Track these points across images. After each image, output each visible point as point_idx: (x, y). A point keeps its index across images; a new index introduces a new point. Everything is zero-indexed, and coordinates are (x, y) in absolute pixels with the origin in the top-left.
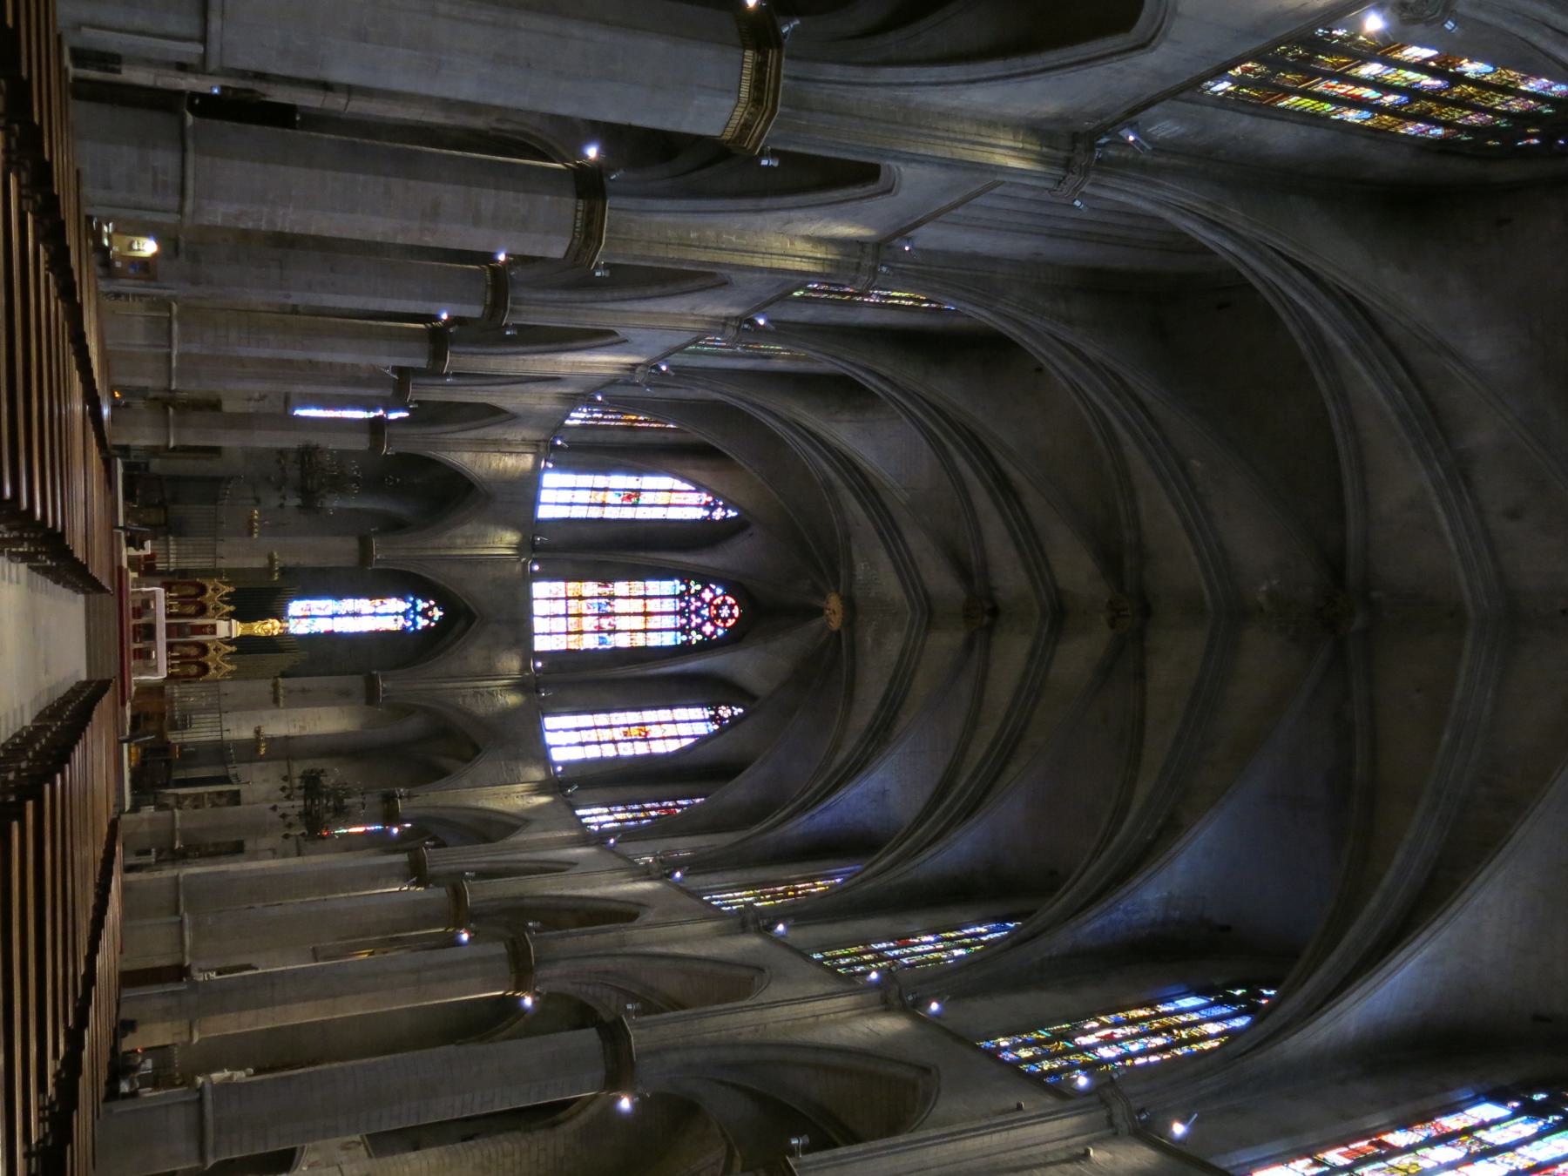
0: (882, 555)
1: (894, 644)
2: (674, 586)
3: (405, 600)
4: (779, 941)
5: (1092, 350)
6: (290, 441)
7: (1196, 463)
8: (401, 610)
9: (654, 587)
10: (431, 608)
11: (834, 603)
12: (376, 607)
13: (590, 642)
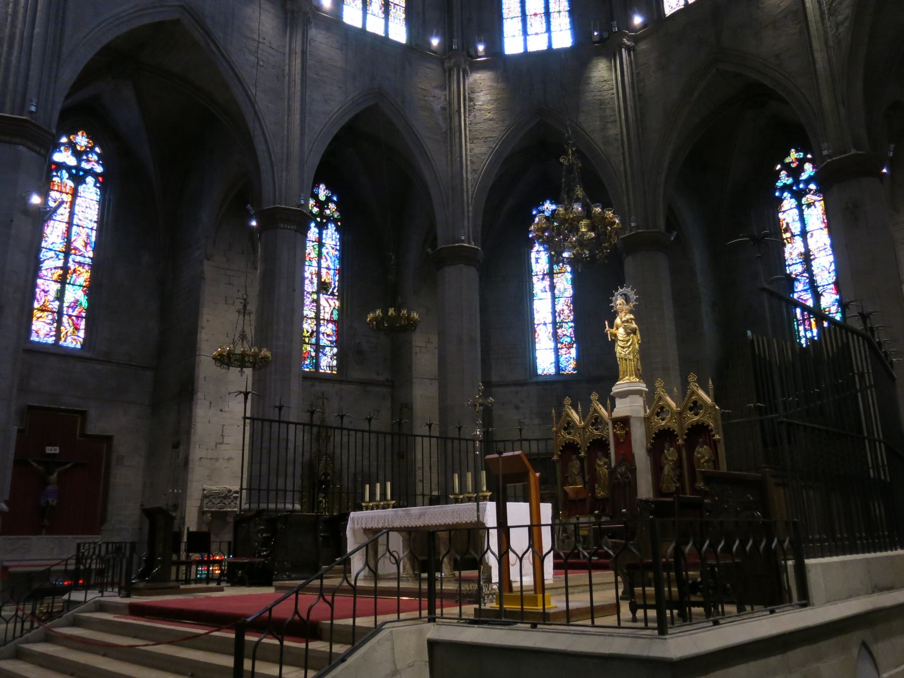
3: (780, 200)
8: (793, 202)
10: (786, 167)
12: (793, 236)
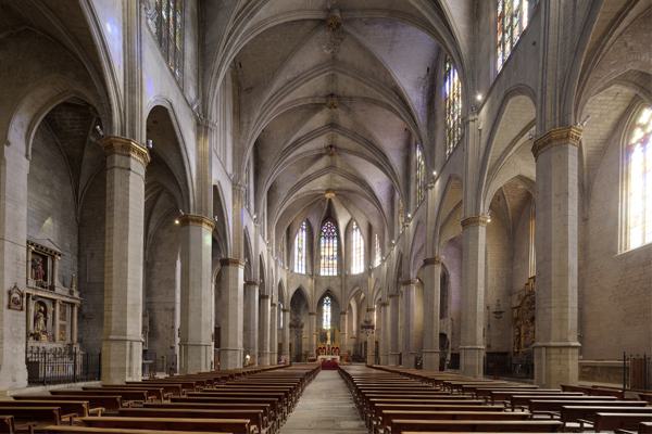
0: (315, 181)
1: (339, 178)
2: (322, 241)
4: (413, 216)
5: (257, 115)
6: (288, 329)
7: (288, 77)
9: (323, 245)
11: (328, 196)
13: (335, 262)
